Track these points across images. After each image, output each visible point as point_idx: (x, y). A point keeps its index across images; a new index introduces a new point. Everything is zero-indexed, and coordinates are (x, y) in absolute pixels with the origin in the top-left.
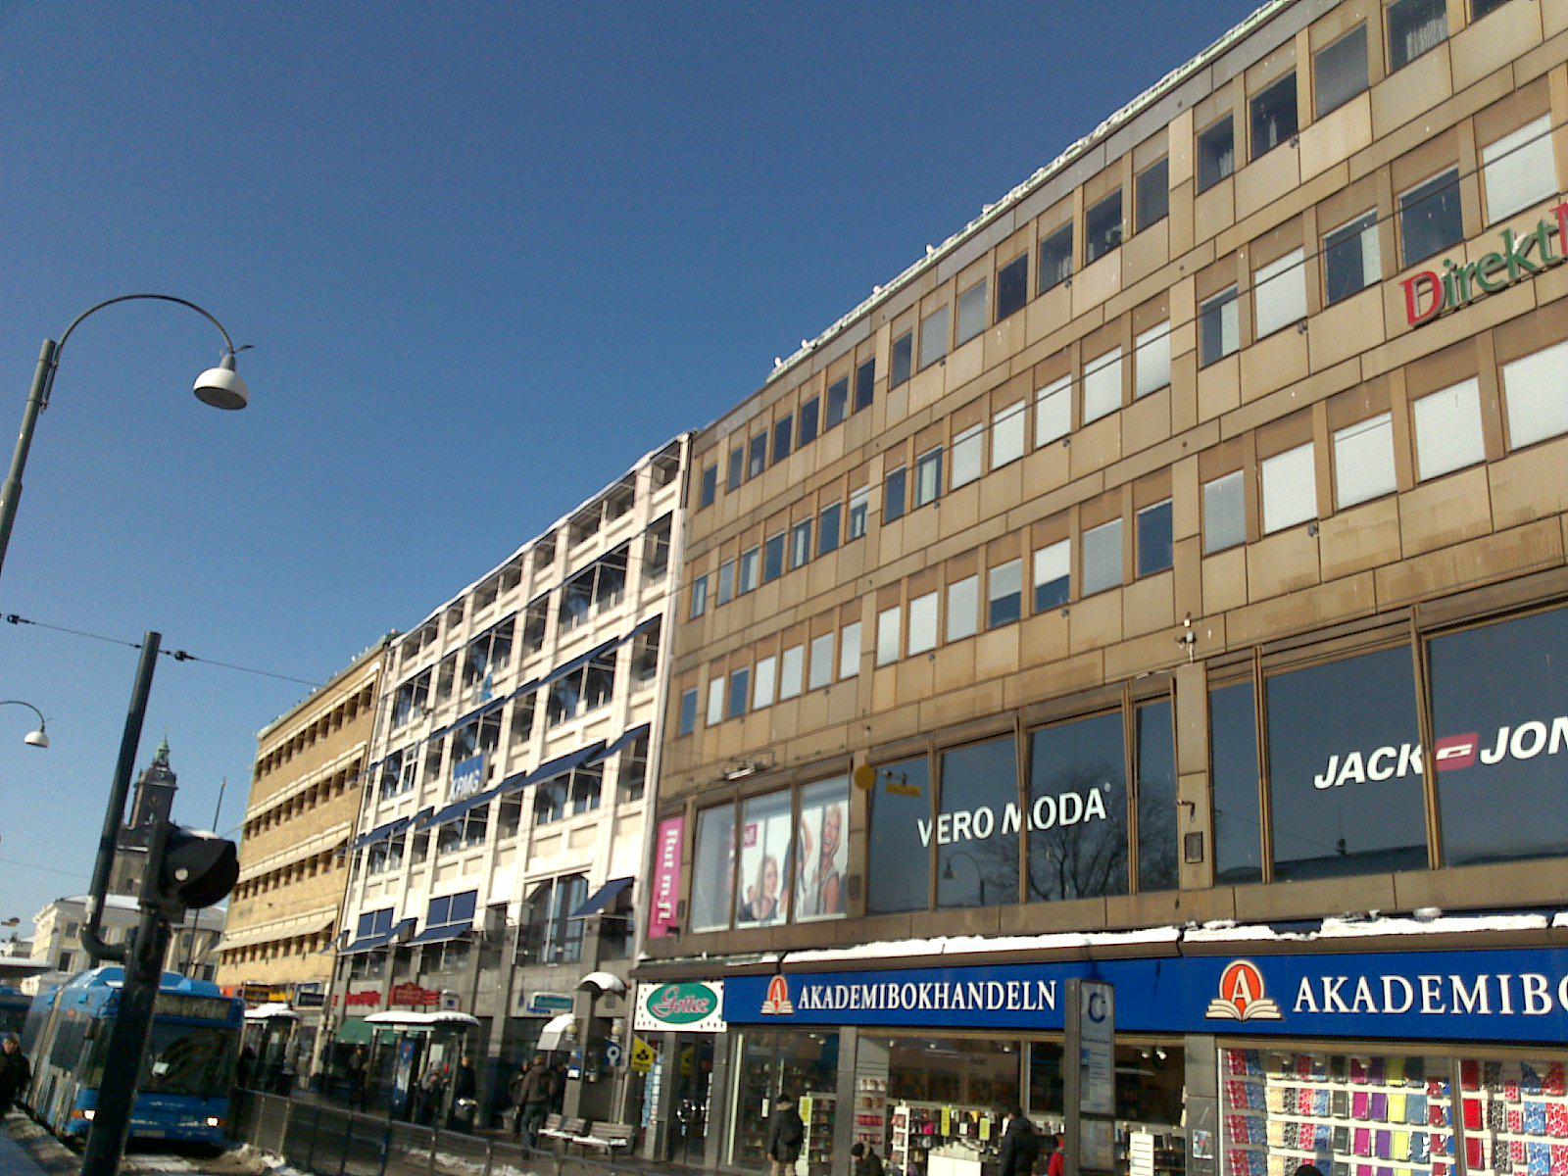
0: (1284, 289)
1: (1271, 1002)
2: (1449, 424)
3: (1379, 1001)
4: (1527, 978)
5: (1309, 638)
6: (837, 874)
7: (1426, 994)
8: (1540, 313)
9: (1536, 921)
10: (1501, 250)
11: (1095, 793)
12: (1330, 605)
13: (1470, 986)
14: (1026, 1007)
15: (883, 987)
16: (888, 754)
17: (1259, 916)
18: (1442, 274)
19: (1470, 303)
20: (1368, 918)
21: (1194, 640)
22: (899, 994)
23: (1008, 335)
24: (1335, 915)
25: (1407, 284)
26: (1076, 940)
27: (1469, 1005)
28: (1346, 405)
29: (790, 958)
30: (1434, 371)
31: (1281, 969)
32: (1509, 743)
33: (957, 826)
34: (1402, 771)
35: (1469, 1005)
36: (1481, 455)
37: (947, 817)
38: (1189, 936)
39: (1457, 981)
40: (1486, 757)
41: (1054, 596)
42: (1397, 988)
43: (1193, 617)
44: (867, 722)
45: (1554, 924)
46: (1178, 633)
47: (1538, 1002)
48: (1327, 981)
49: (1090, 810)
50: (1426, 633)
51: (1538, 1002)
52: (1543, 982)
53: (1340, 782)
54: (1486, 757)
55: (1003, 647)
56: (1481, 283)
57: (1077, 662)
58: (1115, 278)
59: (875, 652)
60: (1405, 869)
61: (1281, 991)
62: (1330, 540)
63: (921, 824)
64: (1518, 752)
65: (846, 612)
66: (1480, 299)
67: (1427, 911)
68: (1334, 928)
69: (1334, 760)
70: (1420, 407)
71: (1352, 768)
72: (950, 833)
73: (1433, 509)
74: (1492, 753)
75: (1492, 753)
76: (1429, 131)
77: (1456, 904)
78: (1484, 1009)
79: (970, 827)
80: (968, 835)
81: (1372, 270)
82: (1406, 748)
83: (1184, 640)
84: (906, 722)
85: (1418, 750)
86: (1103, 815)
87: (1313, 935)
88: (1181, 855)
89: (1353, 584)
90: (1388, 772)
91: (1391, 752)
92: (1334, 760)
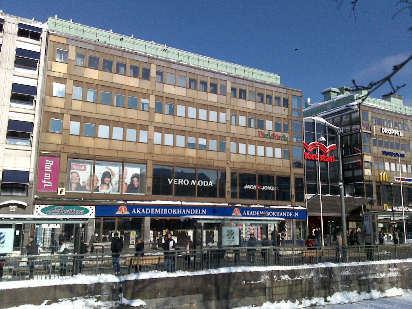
0: (242, 120)
6: (126, 184)
12: (248, 166)
13: (262, 212)
15: (162, 210)
26: (213, 204)
29: (128, 202)
37: (177, 179)
46: (227, 163)
55: (191, 153)
57: (209, 161)
65: (144, 127)
72: (178, 182)
76: (261, 113)
79: (183, 182)
86: (212, 185)
89: (250, 165)
90: (252, 188)
92: (246, 185)
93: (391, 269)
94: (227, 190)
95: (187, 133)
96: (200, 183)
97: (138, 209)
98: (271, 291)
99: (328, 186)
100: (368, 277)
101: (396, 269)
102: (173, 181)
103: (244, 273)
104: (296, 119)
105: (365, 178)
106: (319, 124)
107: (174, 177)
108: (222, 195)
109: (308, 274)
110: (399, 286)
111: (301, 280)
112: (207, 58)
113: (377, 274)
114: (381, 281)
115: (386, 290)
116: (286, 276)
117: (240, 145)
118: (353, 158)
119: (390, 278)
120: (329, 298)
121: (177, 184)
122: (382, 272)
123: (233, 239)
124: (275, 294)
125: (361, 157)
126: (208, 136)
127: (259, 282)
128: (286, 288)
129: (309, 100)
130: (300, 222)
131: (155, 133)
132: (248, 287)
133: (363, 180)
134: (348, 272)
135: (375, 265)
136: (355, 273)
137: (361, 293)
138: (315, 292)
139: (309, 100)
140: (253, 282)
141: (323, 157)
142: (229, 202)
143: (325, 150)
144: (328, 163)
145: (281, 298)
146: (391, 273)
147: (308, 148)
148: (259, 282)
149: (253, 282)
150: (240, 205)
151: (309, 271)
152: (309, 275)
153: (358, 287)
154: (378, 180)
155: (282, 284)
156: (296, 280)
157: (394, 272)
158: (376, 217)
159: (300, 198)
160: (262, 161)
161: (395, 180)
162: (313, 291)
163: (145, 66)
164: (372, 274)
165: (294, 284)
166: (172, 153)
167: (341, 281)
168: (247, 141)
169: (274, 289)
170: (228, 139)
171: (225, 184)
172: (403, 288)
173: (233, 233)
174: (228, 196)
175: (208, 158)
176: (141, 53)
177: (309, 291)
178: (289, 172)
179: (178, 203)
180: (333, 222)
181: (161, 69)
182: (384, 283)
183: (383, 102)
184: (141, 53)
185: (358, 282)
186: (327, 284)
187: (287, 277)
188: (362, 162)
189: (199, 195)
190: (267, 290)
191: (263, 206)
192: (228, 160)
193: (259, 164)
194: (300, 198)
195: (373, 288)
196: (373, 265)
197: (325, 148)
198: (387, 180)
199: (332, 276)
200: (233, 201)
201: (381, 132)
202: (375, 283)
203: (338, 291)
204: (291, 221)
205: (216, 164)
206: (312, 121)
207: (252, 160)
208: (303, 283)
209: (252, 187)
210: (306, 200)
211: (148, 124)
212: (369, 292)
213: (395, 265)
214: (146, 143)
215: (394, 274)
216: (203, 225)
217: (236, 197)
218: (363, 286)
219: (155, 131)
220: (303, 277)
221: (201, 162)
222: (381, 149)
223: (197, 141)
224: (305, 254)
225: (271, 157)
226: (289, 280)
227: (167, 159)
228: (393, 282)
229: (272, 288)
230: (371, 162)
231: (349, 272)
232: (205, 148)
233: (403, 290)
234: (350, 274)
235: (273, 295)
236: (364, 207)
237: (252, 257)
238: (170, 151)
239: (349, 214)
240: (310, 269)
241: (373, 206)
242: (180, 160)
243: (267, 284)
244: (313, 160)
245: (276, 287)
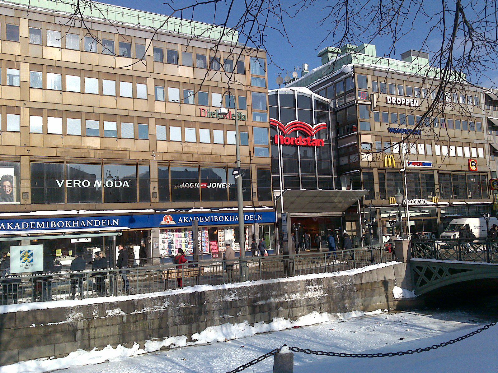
4: (215, 217)
5: (179, 162)
17: (173, 207)
27: (207, 220)
28: (188, 124)
30: (205, 125)
31: (175, 216)
32: (211, 185)
35: (207, 220)
39: (205, 217)
44: (28, 148)
49: (124, 185)
52: (217, 217)
54: (208, 186)
60: (195, 201)
63: (58, 181)
78: (209, 221)
85: (198, 184)
86: (128, 186)
92: (183, 183)
93: (310, 287)
94: (152, 191)
95: (83, 115)
96: (86, 184)
97: (67, 222)
98: (86, 333)
99: (299, 177)
100: (268, 301)
101: (320, 286)
102: (65, 183)
103: (33, 312)
104: (257, 90)
105: (362, 165)
106: (302, 97)
107: (66, 177)
108: (145, 196)
109: (159, 304)
110: (323, 309)
111: (145, 315)
112: (120, 9)
113: (286, 295)
114: (293, 304)
115: (300, 316)
116: (117, 311)
117: (172, 128)
118: (347, 139)
119: (308, 299)
120: (195, 336)
122: (295, 293)
123: (30, 263)
124: (94, 338)
125: (357, 137)
126: (119, 119)
127: (63, 322)
128: (116, 329)
129: (306, 66)
130: (267, 226)
131: (32, 118)
132: (42, 331)
133: (359, 167)
134: (233, 296)
135: (283, 283)
136: (246, 297)
137: (256, 324)
138: (171, 329)
139: (306, 66)
140: (51, 324)
141: (306, 141)
142: (155, 207)
143: (310, 130)
144: (315, 148)
145: (105, 342)
146: (310, 293)
147: (285, 130)
148: (63, 322)
149: (51, 324)
150: (173, 210)
151: (162, 300)
152: (161, 305)
153: (249, 317)
154: (382, 166)
155: (106, 323)
156: (136, 315)
157: (317, 290)
158: (378, 215)
159: (265, 195)
160: (207, 149)
161: (407, 164)
162: (167, 327)
163: (11, 22)
164: (276, 296)
165: (131, 320)
166: (60, 145)
167: (220, 309)
168: (183, 122)
169: (92, 331)
170: (152, 122)
171: (150, 184)
172: (329, 312)
173: (32, 255)
174: (155, 200)
175: (120, 149)
176: (10, 4)
177: (160, 328)
179: (74, 212)
180: (300, 224)
181: (37, 26)
182: (298, 307)
183: (401, 63)
184: (10, 4)
185: (251, 308)
186: (193, 316)
187: (118, 312)
188: (358, 143)
189: (107, 200)
190: (79, 334)
191: (209, 210)
192: (153, 151)
193: (202, 154)
194: (265, 195)
195: (278, 316)
196: (279, 283)
197: (309, 128)
198: (395, 166)
199: (204, 304)
200: (161, 205)
201: (387, 103)
202: (281, 309)
203: (212, 324)
204: (253, 226)
205: (133, 156)
206: (292, 93)
207: (192, 148)
208: (149, 317)
210: (275, 197)
211: (18, 104)
212: (269, 321)
213: (318, 281)
214: (132, 139)
215: (315, 293)
216: (114, 238)
217: (168, 200)
218: (258, 315)
219: (30, 115)
220: (148, 310)
221: (108, 155)
222: (385, 126)
223: (101, 126)
224: (167, 276)
225: (218, 144)
226: (122, 316)
227: (53, 153)
228: (314, 305)
229: (88, 329)
230: (371, 143)
231: (236, 296)
232: (117, 135)
233: (329, 315)
234: (237, 298)
235: (89, 340)
236: (361, 202)
237: (77, 286)
238: (58, 141)
239: (344, 213)
240: (163, 297)
241: (373, 201)
242: (74, 153)
243: (79, 325)
244: (293, 146)
245: (95, 327)
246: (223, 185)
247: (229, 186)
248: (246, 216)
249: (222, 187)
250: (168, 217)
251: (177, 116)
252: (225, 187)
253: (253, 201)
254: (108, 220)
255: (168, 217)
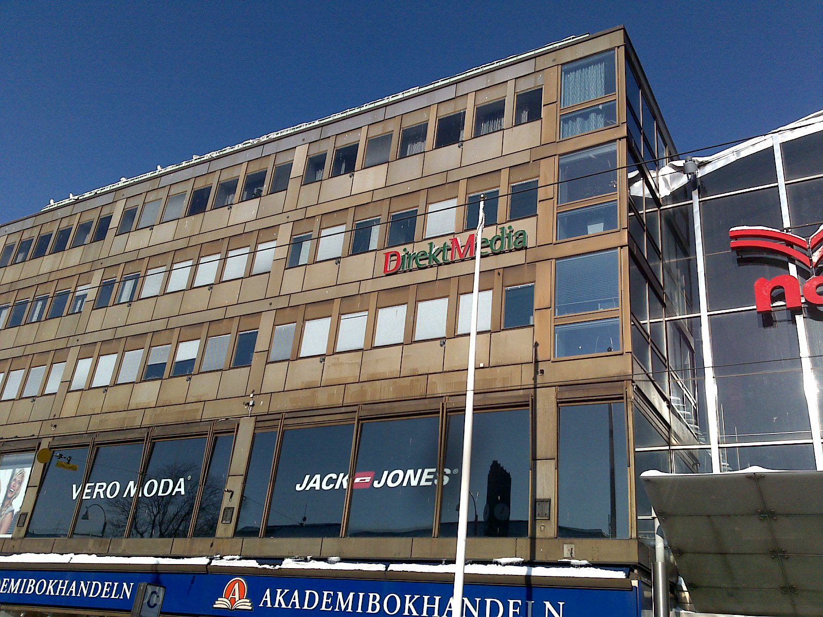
0: (333, 242)
1: (248, 601)
2: (391, 324)
3: (302, 603)
4: (371, 595)
7: (325, 600)
8: (437, 282)
9: (381, 567)
10: (428, 251)
11: (182, 480)
12: (322, 398)
14: (113, 597)
16: (64, 443)
17: (253, 555)
18: (402, 254)
19: (411, 271)
20: (306, 560)
21: (253, 405)
22: (35, 586)
23: (192, 224)
24: (290, 557)
25: (387, 254)
27: (343, 607)
28: (350, 303)
30: (390, 297)
31: (256, 583)
32: (387, 479)
33: (97, 490)
34: (337, 487)
35: (343, 607)
36: (489, 328)
38: (214, 563)
39: (340, 594)
40: (376, 484)
41: (185, 369)
42: (312, 596)
43: (255, 393)
44: (54, 422)
45: (388, 570)
46: (246, 400)
47: (374, 607)
48: (408, 597)
49: (177, 489)
50: (450, 412)
51: (374, 607)
53: (308, 489)
55: (149, 392)
56: (417, 263)
57: (188, 407)
58: (254, 212)
59: (70, 382)
61: (254, 595)
62: (329, 366)
63: (74, 486)
64: (390, 484)
65: (58, 355)
66: (415, 270)
67: (334, 559)
68: (288, 564)
69: (307, 477)
70: (420, 305)
71: (315, 482)
72: (91, 494)
73: (377, 361)
74: (379, 483)
75: (379, 483)
76: (409, 190)
77: (348, 556)
78: (349, 610)
80: (102, 496)
81: (373, 245)
82: (342, 475)
83: (248, 404)
84: (80, 425)
85: (347, 477)
86: (183, 493)
87: (278, 567)
88: (220, 519)
90: (332, 486)
91: (334, 476)
92: (307, 477)
121: (89, 497)
150: (253, 563)
178: (528, 380)
179: (65, 559)
209: (331, 481)
246: (425, 476)
247: (446, 480)
248: (488, 601)
249: (423, 483)
250: (237, 586)
251: (327, 291)
252: (430, 483)
253: (533, 539)
254: (116, 584)
255: (237, 586)
